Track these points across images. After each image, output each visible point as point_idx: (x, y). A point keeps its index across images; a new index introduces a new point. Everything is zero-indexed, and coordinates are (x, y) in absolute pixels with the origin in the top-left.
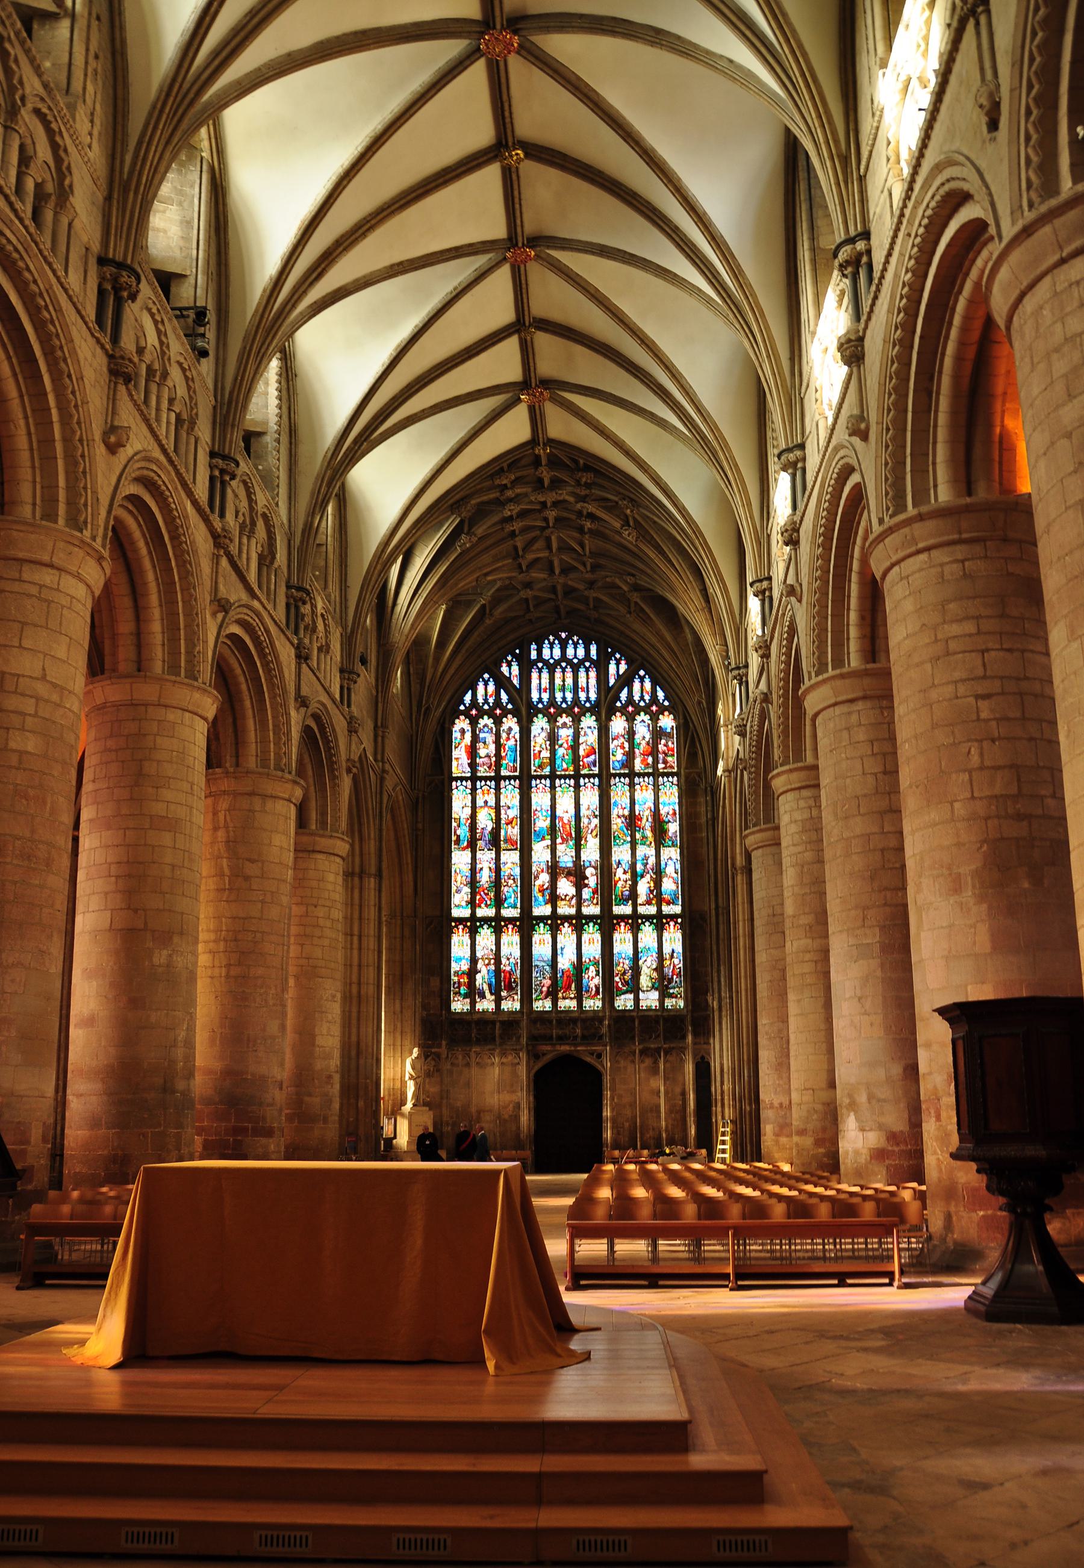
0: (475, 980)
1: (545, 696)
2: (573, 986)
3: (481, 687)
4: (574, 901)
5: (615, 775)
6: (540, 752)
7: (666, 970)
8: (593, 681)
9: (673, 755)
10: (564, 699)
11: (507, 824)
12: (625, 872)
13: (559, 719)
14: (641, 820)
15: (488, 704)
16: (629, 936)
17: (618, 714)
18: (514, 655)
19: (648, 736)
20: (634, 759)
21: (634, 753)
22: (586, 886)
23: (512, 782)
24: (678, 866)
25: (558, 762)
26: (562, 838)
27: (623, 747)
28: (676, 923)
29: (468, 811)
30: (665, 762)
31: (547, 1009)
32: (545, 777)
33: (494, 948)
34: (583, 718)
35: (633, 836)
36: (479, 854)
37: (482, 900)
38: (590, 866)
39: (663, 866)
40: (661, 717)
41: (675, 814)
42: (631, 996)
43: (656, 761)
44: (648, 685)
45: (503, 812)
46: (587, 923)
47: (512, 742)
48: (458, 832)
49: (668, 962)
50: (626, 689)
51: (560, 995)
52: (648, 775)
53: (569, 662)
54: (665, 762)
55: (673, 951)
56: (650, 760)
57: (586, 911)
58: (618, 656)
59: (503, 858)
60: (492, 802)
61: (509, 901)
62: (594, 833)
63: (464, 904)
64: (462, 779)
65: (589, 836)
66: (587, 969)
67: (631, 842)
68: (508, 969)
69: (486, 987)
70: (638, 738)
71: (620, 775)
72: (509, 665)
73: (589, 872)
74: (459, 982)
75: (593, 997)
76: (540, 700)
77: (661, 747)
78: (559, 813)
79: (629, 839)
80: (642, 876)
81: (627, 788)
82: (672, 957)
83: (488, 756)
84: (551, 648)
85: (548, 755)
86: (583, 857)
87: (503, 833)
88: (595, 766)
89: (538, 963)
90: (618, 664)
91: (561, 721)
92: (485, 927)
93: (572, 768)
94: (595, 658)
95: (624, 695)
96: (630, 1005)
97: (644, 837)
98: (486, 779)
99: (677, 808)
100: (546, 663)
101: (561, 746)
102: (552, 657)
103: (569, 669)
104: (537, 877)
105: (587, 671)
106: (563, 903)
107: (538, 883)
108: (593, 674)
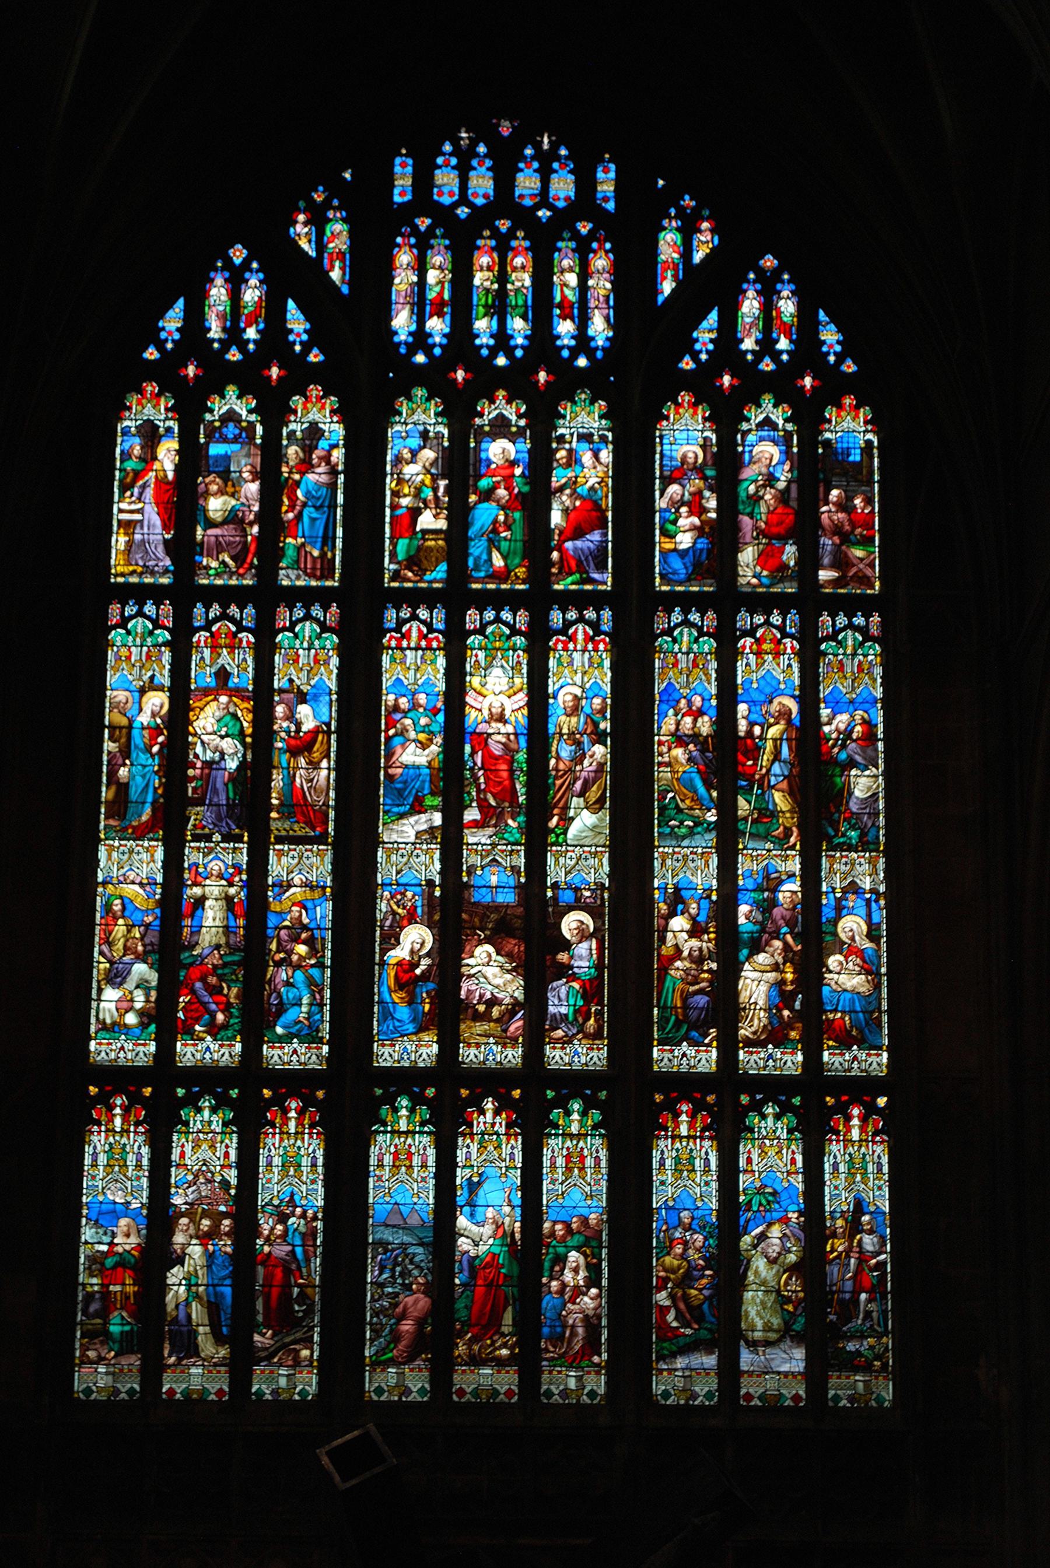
0: (163, 1288)
1: (437, 326)
2: (508, 1318)
3: (218, 293)
4: (516, 1025)
5: (670, 601)
6: (415, 513)
7: (834, 1271)
8: (601, 285)
9: (868, 541)
10: (502, 338)
11: (294, 752)
12: (696, 931)
13: (483, 405)
14: (755, 752)
15: (242, 345)
16: (708, 1151)
17: (685, 397)
18: (335, 188)
19: (783, 476)
20: (735, 548)
21: (736, 528)
22: (565, 971)
23: (317, 611)
24: (879, 915)
25: (477, 549)
26: (483, 806)
27: (696, 507)
28: (870, 1109)
29: (157, 701)
30: (841, 562)
31: (414, 1397)
32: (428, 598)
33: (232, 1176)
34: (566, 409)
35: (726, 808)
36: (192, 855)
37: (198, 1010)
38: (578, 905)
39: (828, 913)
40: (830, 412)
41: (869, 736)
42: (710, 1361)
43: (809, 561)
44: (787, 307)
45: (280, 710)
46: (562, 1103)
47: (317, 477)
48: (123, 772)
49: (841, 1246)
50: (713, 316)
51: (461, 1349)
52: (783, 603)
53: (523, 217)
54: (841, 562)
55: (859, 1207)
56: (790, 553)
57: (556, 1057)
58: (687, 201)
59: (278, 866)
60: (244, 677)
61: (291, 1015)
62: (593, 794)
63: (131, 1019)
64: (140, 594)
65: (575, 801)
66: (561, 1260)
67: (718, 826)
68: (281, 1251)
69: (197, 1311)
70: (749, 484)
71: (687, 602)
72: (318, 221)
73: (570, 924)
74: (105, 1294)
75: (574, 1361)
76: (420, 338)
77: (828, 513)
78: (472, 717)
79: (711, 817)
80: (757, 947)
81: (708, 644)
82: (854, 1227)
83: (233, 519)
84: (464, 171)
85: (442, 524)
86: (556, 871)
87: (278, 780)
88: (602, 567)
89: (387, 1235)
90: (688, 232)
91: (489, 412)
92: (206, 1103)
93: (521, 572)
94: (611, 206)
95: (705, 334)
96: (705, 1388)
97: (766, 814)
98: (225, 596)
99: (878, 717)
100: (443, 215)
101: (487, 496)
102: (464, 199)
103: (520, 242)
104: (392, 939)
105: (583, 252)
106: (480, 1027)
107: (400, 953)
108: (600, 262)
